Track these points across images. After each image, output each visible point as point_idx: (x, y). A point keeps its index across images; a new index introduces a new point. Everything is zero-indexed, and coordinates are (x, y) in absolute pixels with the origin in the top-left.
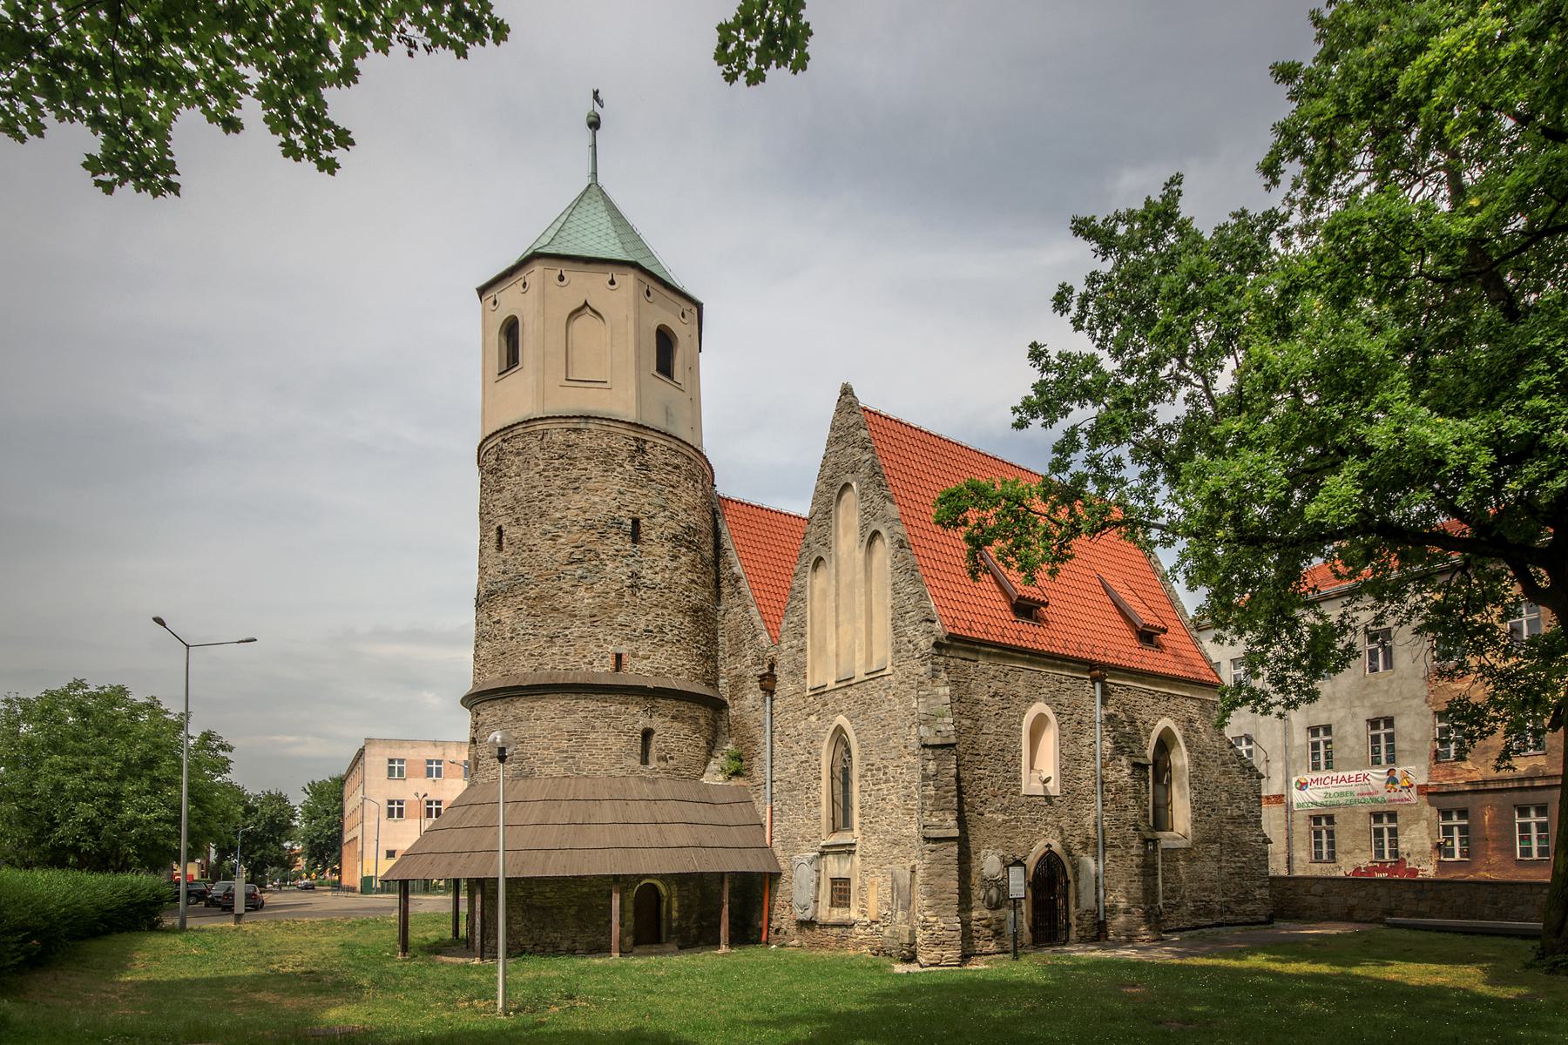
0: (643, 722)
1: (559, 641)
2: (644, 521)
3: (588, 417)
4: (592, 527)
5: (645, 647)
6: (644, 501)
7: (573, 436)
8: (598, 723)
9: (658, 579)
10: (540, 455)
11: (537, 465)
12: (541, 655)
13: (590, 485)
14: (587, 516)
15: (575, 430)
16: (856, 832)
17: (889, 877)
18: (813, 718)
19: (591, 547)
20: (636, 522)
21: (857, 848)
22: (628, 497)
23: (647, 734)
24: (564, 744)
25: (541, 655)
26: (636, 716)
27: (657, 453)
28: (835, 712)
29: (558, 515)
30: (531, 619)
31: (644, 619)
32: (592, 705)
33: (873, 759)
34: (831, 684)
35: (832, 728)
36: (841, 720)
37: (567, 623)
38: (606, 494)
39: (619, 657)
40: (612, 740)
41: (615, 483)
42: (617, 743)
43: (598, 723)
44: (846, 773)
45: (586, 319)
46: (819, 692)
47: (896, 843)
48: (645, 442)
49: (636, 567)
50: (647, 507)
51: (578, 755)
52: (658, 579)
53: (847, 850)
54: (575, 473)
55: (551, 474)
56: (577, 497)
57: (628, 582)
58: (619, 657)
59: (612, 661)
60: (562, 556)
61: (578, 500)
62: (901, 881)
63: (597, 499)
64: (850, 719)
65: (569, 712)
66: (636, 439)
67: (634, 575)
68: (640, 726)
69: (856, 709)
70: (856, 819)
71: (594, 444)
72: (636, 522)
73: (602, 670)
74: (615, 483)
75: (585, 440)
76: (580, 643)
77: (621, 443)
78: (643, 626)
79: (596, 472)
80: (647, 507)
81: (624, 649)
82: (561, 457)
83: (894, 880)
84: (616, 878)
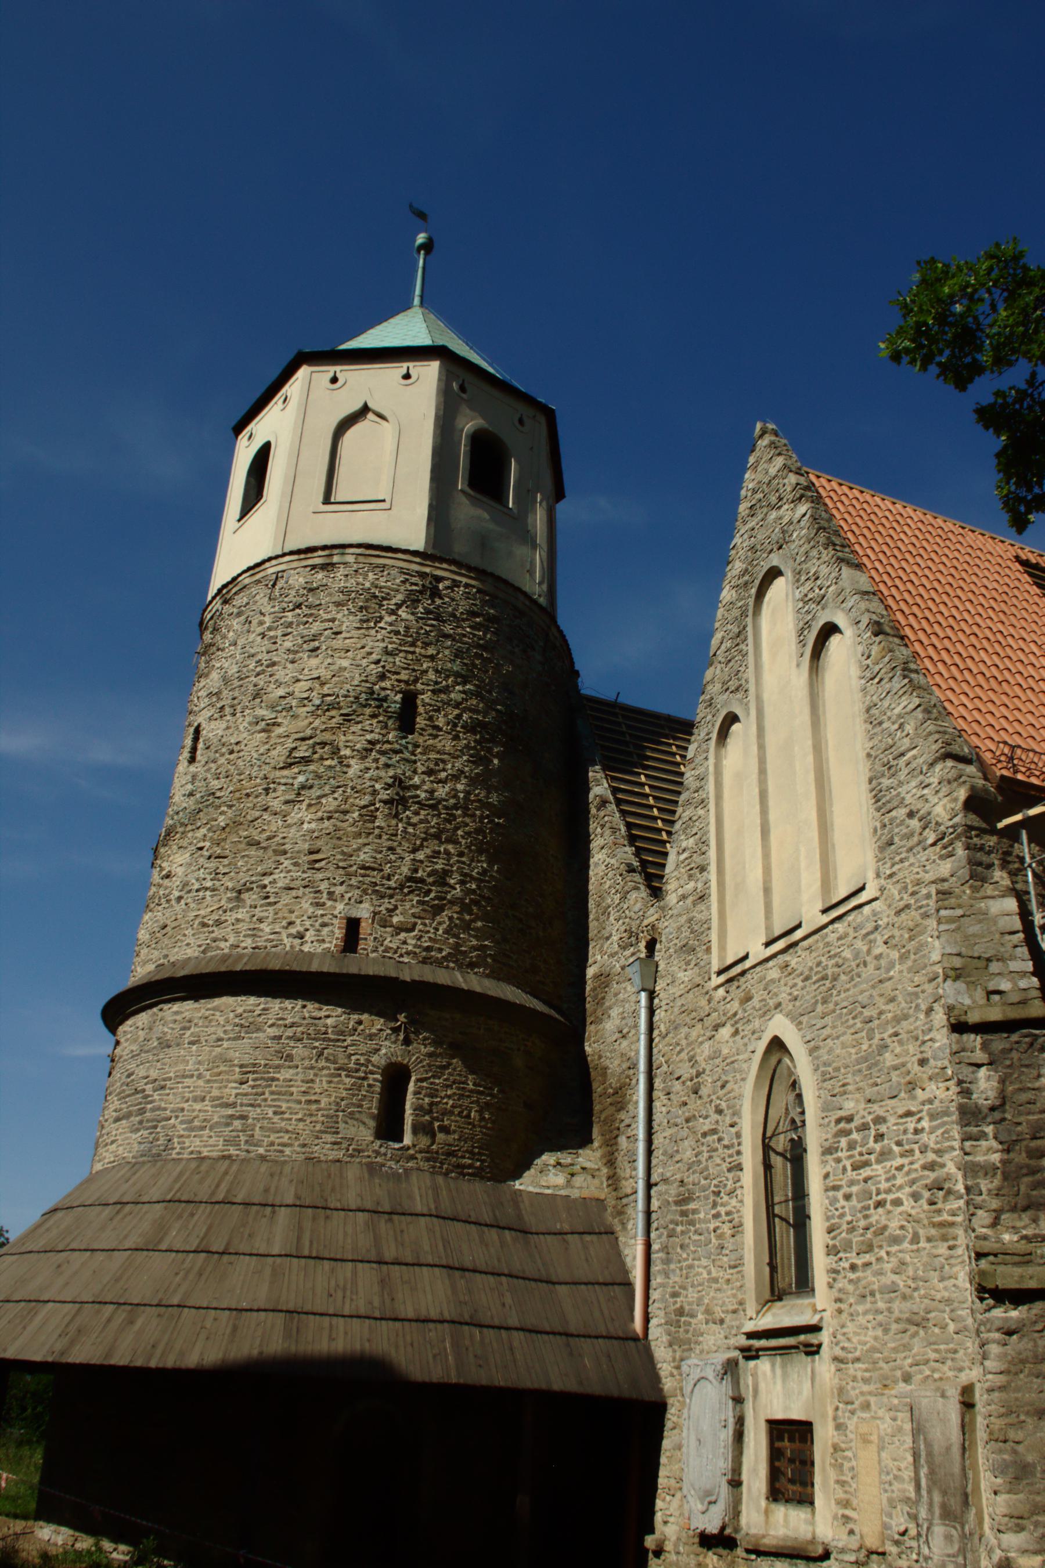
0: (389, 1050)
1: (249, 898)
4: (331, 707)
9: (442, 792)
10: (267, 609)
11: (261, 623)
12: (218, 923)
13: (338, 643)
14: (326, 690)
15: (324, 567)
16: (822, 1295)
17: (904, 1416)
18: (725, 1032)
19: (327, 737)
20: (410, 700)
21: (824, 1337)
23: (395, 1078)
25: (218, 923)
28: (766, 1013)
29: (281, 692)
30: (212, 864)
31: (408, 857)
33: (849, 1106)
34: (758, 952)
35: (762, 1046)
36: (780, 1026)
37: (269, 864)
43: (298, 1050)
44: (797, 1155)
46: (734, 973)
47: (917, 1322)
48: (439, 579)
51: (253, 1113)
52: (442, 792)
53: (799, 1341)
54: (316, 627)
55: (279, 633)
56: (314, 662)
57: (384, 795)
58: (353, 925)
59: (338, 932)
62: (936, 1434)
63: (345, 663)
64: (796, 1019)
65: (252, 1027)
66: (422, 575)
67: (398, 782)
69: (809, 993)
70: (820, 1262)
72: (410, 700)
75: (339, 579)
76: (286, 899)
81: (363, 912)
82: (299, 606)
83: (918, 1431)
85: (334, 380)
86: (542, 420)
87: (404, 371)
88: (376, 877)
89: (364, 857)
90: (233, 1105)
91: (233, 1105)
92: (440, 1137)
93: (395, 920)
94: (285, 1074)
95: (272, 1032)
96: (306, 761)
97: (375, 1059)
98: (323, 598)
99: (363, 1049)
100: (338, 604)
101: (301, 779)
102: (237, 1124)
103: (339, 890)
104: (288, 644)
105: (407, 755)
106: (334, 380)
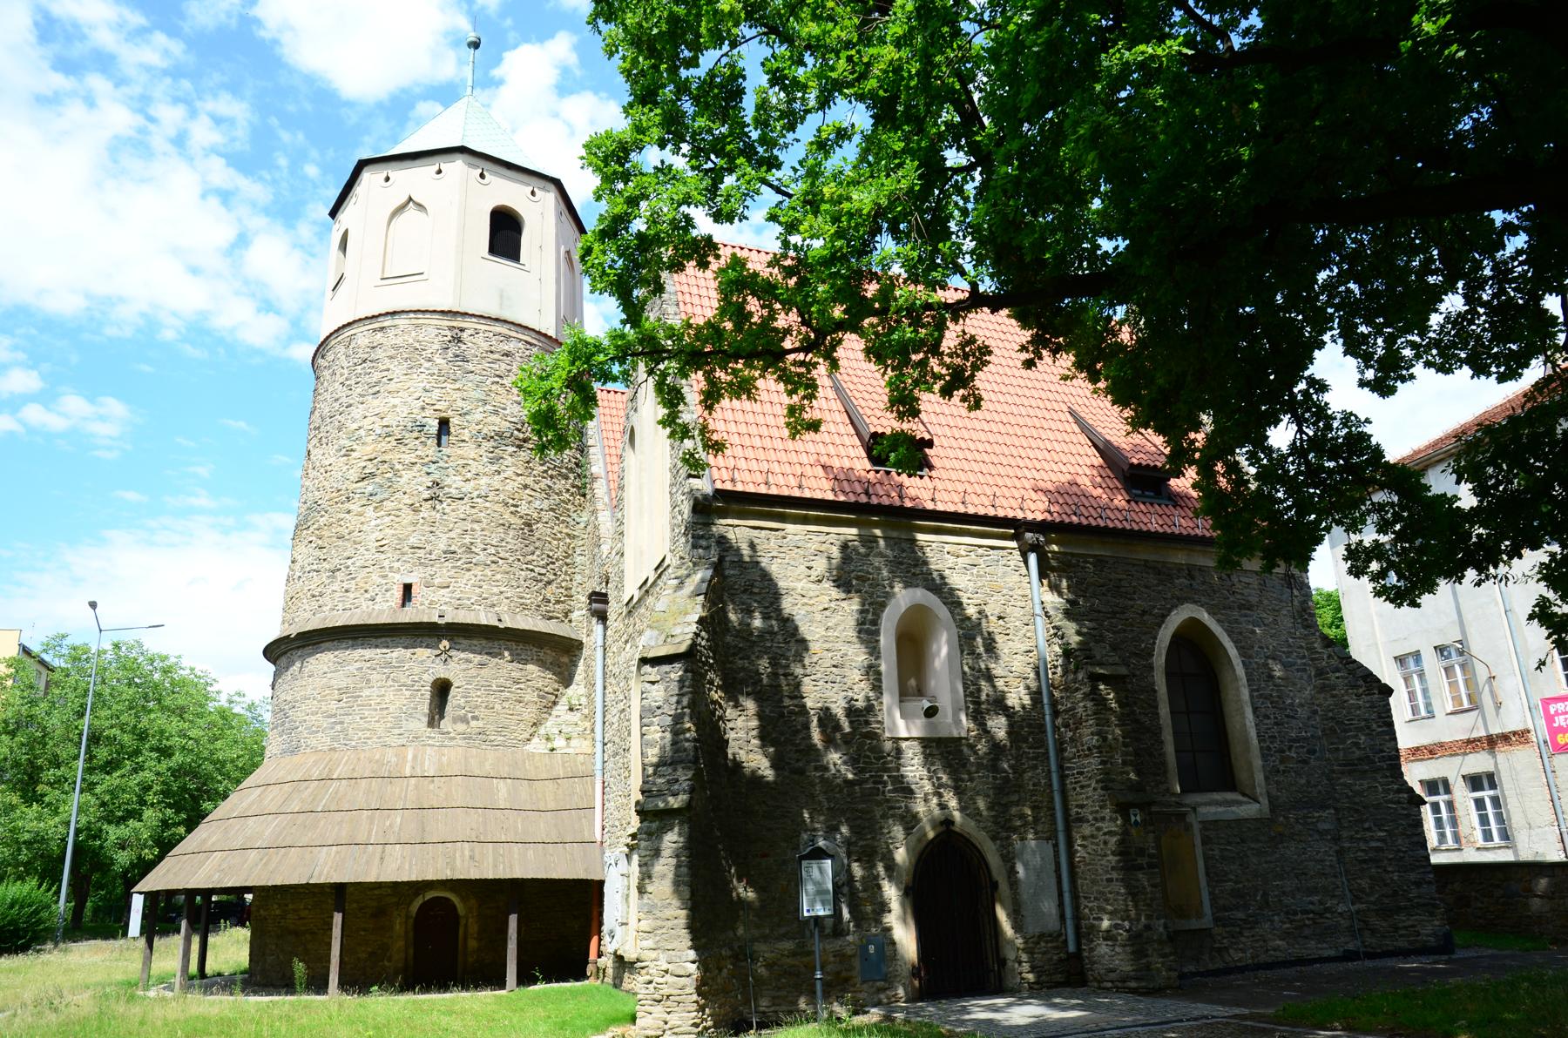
2: (454, 421)
3: (394, 313)
5: (443, 573)
6: (448, 399)
7: (380, 334)
8: (375, 676)
9: (468, 487)
10: (345, 364)
13: (392, 386)
19: (386, 458)
20: (444, 424)
22: (436, 394)
23: (442, 690)
24: (333, 706)
26: (424, 663)
27: (478, 341)
29: (355, 426)
30: (317, 553)
31: (444, 537)
32: (368, 653)
38: (407, 396)
39: (407, 588)
40: (390, 696)
41: (419, 382)
42: (397, 700)
43: (375, 676)
45: (411, 210)
48: (462, 330)
49: (436, 477)
50: (460, 403)
51: (347, 719)
52: (468, 487)
54: (376, 376)
55: (352, 382)
56: (376, 402)
58: (407, 588)
59: (398, 593)
60: (354, 474)
61: (375, 404)
63: (397, 401)
66: (451, 328)
68: (429, 679)
71: (399, 341)
72: (444, 424)
73: (386, 610)
74: (419, 382)
75: (390, 339)
77: (432, 333)
78: (442, 547)
79: (398, 370)
80: (460, 403)
84: (340, 889)
85: (387, 179)
86: (552, 187)
87: (436, 168)
88: (421, 553)
89: (413, 541)
90: (335, 715)
91: (335, 715)
92: (473, 723)
93: (436, 582)
94: (366, 692)
95: (358, 665)
96: (373, 475)
97: (425, 677)
98: (379, 353)
99: (417, 671)
100: (391, 358)
101: (370, 488)
102: (338, 727)
103: (396, 565)
104: (359, 390)
105: (442, 464)
106: (387, 179)
